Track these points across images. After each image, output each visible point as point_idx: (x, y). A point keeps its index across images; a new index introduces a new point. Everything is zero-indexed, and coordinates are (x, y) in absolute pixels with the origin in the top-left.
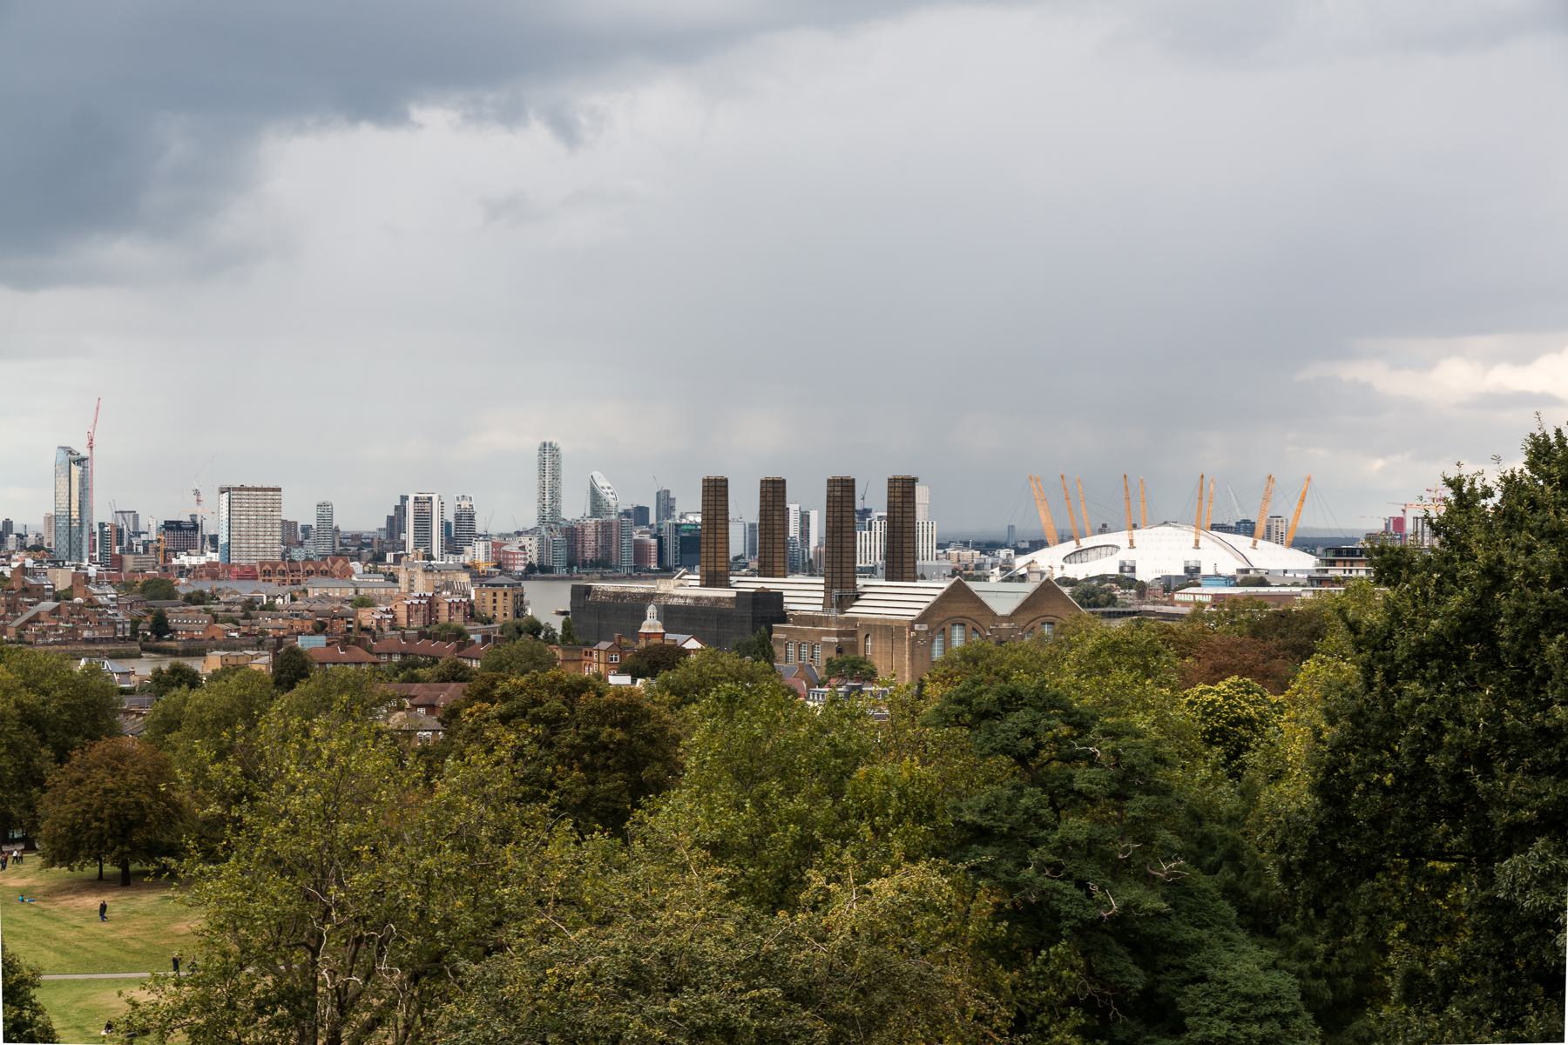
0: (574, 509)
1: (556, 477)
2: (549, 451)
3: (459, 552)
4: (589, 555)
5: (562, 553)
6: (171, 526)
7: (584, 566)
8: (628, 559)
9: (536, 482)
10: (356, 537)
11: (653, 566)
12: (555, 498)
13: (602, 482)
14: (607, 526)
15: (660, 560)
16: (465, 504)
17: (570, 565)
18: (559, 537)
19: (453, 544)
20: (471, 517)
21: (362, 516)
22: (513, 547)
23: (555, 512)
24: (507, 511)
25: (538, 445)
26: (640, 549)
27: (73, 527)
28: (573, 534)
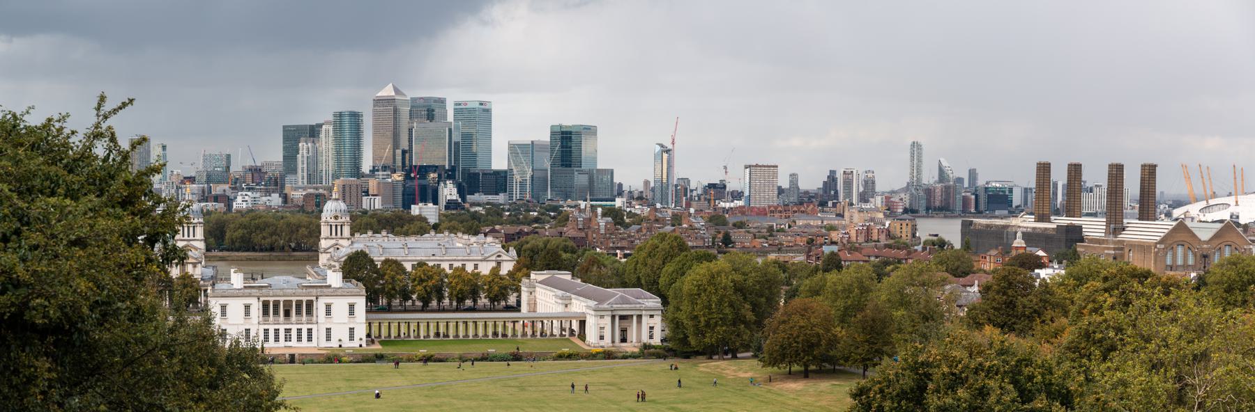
0: (929, 177)
1: (920, 161)
2: (916, 148)
3: (866, 201)
4: (937, 204)
5: (923, 203)
6: (712, 186)
7: (935, 209)
8: (959, 206)
9: (909, 163)
10: (807, 192)
11: (973, 210)
12: (919, 172)
13: (945, 164)
14: (947, 188)
15: (976, 207)
16: (870, 175)
17: (928, 209)
18: (922, 193)
19: (864, 198)
20: (873, 183)
21: (812, 182)
22: (895, 199)
23: (919, 180)
24: (892, 178)
25: (910, 142)
26: (965, 201)
27: (663, 187)
28: (929, 192)
